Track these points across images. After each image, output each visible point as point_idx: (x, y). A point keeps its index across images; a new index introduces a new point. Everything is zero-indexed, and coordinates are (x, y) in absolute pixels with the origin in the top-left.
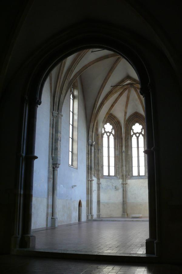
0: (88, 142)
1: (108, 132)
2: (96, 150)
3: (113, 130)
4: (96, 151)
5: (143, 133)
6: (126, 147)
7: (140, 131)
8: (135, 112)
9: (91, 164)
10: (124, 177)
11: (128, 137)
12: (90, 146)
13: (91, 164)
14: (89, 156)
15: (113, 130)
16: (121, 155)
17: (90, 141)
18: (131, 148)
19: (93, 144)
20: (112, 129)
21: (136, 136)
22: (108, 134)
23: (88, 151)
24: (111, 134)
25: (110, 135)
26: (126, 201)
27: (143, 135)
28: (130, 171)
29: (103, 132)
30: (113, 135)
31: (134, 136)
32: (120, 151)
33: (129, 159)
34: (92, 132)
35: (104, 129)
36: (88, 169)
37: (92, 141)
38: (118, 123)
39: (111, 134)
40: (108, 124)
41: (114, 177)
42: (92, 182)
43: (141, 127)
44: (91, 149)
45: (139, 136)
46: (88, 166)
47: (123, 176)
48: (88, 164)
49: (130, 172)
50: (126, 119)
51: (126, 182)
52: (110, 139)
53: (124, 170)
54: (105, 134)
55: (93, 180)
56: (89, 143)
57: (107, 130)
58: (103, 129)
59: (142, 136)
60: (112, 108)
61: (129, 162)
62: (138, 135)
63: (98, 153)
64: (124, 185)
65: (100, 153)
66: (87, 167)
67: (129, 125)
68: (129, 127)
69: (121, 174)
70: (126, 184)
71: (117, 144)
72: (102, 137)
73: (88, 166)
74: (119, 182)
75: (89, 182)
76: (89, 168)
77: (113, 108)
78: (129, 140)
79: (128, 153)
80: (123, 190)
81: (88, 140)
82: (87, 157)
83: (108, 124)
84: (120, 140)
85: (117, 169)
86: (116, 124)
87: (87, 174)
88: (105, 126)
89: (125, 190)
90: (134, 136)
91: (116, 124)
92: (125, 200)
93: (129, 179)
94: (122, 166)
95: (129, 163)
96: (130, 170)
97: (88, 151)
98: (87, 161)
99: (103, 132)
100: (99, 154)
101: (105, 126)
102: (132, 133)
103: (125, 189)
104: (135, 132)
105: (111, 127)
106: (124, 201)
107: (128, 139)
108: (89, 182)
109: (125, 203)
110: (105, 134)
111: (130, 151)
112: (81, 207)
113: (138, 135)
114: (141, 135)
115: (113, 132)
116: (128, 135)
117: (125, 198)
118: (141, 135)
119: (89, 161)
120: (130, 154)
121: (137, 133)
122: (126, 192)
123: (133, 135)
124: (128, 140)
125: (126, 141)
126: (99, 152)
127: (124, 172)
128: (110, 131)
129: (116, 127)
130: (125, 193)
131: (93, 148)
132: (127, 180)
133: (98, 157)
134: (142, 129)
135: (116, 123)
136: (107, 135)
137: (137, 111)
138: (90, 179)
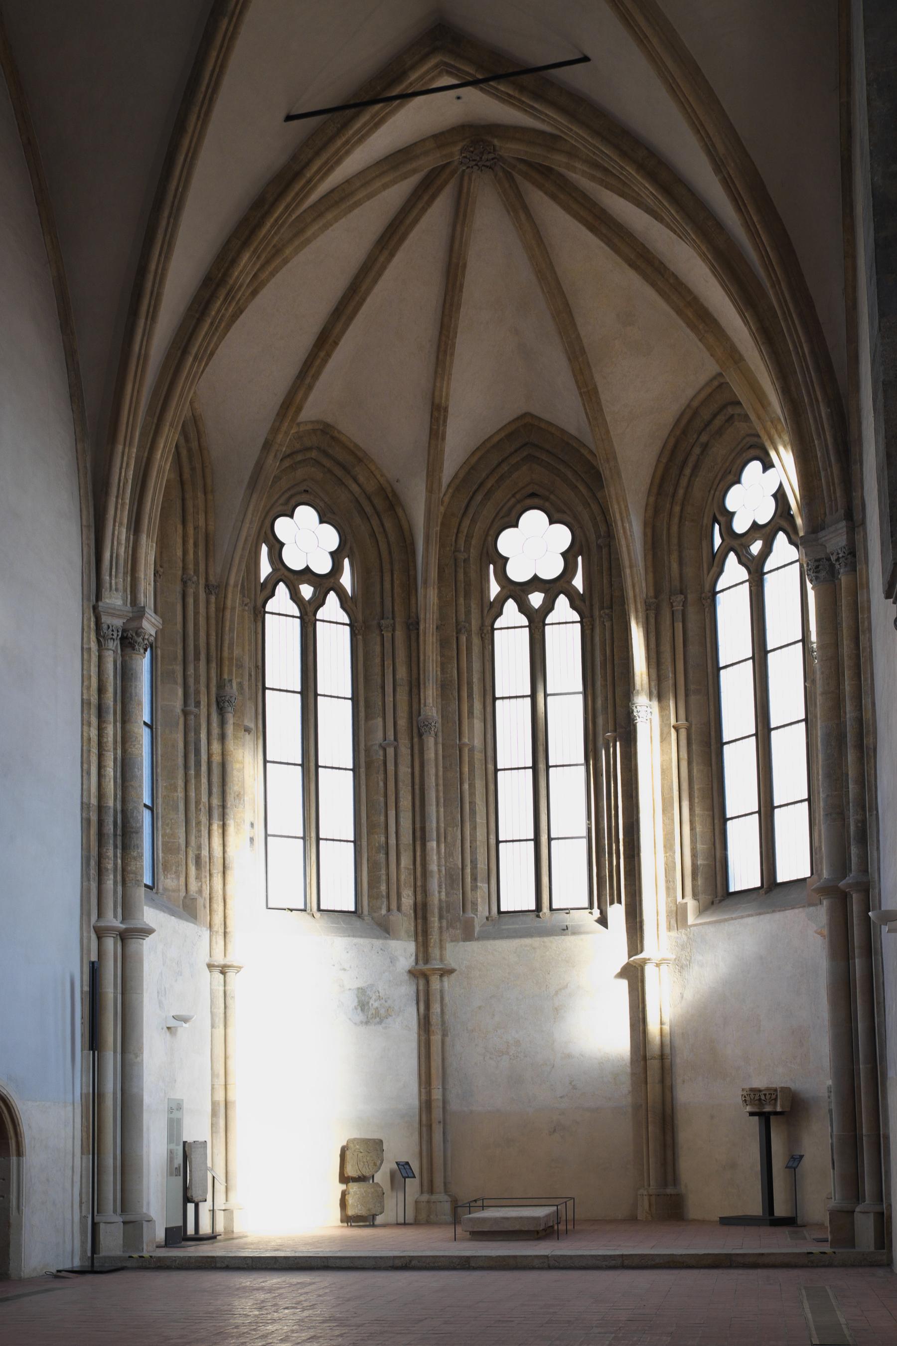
0: (95, 608)
1: (307, 574)
2: (198, 704)
3: (346, 562)
4: (197, 717)
5: (578, 582)
6: (444, 687)
7: (552, 569)
8: (509, 415)
9: (124, 801)
10: (434, 921)
11: (462, 617)
12: (113, 645)
13: (124, 801)
14: (110, 730)
15: (346, 562)
16: (404, 751)
17: (115, 600)
18: (490, 698)
19: (138, 631)
20: (336, 556)
21: (524, 608)
22: (307, 591)
23: (101, 690)
24: (332, 598)
25: (319, 601)
26: (445, 1102)
27: (575, 602)
28: (474, 879)
29: (265, 569)
30: (345, 602)
31: (511, 606)
32: (402, 723)
33: (472, 786)
34: (136, 526)
35: (276, 547)
36: (101, 835)
37: (134, 601)
38: (378, 502)
39: (332, 598)
40: (306, 514)
41: (354, 918)
42: (133, 944)
43: (562, 536)
44: (126, 675)
45: (548, 606)
46: (101, 808)
47: (421, 912)
48: (101, 796)
49: (475, 888)
50: (445, 480)
51: (442, 960)
52: (321, 629)
53: (433, 867)
54: (282, 590)
55: (148, 931)
56: (106, 620)
57: (293, 560)
58: (264, 549)
59: (573, 606)
60: (325, 361)
61: (472, 803)
62: (536, 599)
63: (216, 731)
64: (428, 982)
65: (230, 729)
66: (86, 823)
67: (473, 521)
68: (469, 537)
69: (407, 901)
70: (446, 972)
71: (377, 670)
72: (259, 614)
73: (101, 808)
74: (393, 960)
75: (110, 943)
76: (109, 828)
77: (329, 355)
78: (469, 641)
79: (466, 740)
80: (425, 1024)
81: (98, 597)
82: (85, 741)
83: (306, 514)
84: (399, 634)
85: (382, 856)
86: (368, 509)
87: (85, 875)
88: (283, 527)
89: (435, 1019)
90: (511, 606)
91: (368, 509)
92: (437, 1094)
93: (468, 935)
94: (420, 835)
95: (473, 812)
96: (482, 865)
97: (101, 690)
98: (85, 773)
99: (265, 569)
100: (223, 737)
101: (283, 527)
102: (494, 589)
103: (436, 1008)
104: (518, 573)
105: (330, 538)
106: (426, 1105)
107: (458, 632)
108: (110, 943)
109: (437, 1113)
110: (282, 590)
111: (478, 724)
112: (19, 1153)
113: (536, 599)
114: (562, 601)
115: (346, 580)
116: (461, 600)
117: (436, 1083)
118: (562, 601)
119: (110, 771)
120: (478, 742)
121: (536, 583)
122: (444, 1035)
123: (501, 601)
124: (463, 638)
125: (443, 643)
126: (223, 723)
127: (434, 884)
128: (323, 566)
129: (373, 535)
130: (436, 1038)
131: (144, 664)
132: (454, 940)
133: (217, 759)
134: (568, 556)
135: (369, 498)
136: (295, 596)
137: (537, 411)
138: (113, 920)
